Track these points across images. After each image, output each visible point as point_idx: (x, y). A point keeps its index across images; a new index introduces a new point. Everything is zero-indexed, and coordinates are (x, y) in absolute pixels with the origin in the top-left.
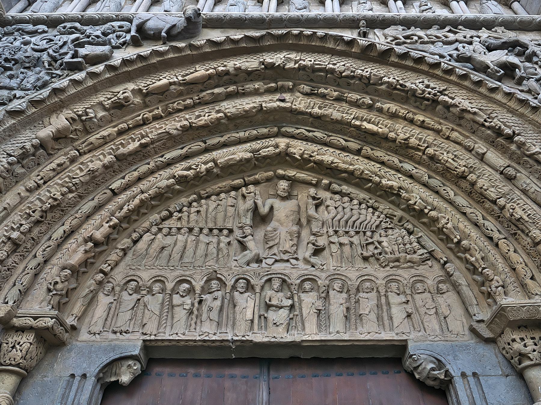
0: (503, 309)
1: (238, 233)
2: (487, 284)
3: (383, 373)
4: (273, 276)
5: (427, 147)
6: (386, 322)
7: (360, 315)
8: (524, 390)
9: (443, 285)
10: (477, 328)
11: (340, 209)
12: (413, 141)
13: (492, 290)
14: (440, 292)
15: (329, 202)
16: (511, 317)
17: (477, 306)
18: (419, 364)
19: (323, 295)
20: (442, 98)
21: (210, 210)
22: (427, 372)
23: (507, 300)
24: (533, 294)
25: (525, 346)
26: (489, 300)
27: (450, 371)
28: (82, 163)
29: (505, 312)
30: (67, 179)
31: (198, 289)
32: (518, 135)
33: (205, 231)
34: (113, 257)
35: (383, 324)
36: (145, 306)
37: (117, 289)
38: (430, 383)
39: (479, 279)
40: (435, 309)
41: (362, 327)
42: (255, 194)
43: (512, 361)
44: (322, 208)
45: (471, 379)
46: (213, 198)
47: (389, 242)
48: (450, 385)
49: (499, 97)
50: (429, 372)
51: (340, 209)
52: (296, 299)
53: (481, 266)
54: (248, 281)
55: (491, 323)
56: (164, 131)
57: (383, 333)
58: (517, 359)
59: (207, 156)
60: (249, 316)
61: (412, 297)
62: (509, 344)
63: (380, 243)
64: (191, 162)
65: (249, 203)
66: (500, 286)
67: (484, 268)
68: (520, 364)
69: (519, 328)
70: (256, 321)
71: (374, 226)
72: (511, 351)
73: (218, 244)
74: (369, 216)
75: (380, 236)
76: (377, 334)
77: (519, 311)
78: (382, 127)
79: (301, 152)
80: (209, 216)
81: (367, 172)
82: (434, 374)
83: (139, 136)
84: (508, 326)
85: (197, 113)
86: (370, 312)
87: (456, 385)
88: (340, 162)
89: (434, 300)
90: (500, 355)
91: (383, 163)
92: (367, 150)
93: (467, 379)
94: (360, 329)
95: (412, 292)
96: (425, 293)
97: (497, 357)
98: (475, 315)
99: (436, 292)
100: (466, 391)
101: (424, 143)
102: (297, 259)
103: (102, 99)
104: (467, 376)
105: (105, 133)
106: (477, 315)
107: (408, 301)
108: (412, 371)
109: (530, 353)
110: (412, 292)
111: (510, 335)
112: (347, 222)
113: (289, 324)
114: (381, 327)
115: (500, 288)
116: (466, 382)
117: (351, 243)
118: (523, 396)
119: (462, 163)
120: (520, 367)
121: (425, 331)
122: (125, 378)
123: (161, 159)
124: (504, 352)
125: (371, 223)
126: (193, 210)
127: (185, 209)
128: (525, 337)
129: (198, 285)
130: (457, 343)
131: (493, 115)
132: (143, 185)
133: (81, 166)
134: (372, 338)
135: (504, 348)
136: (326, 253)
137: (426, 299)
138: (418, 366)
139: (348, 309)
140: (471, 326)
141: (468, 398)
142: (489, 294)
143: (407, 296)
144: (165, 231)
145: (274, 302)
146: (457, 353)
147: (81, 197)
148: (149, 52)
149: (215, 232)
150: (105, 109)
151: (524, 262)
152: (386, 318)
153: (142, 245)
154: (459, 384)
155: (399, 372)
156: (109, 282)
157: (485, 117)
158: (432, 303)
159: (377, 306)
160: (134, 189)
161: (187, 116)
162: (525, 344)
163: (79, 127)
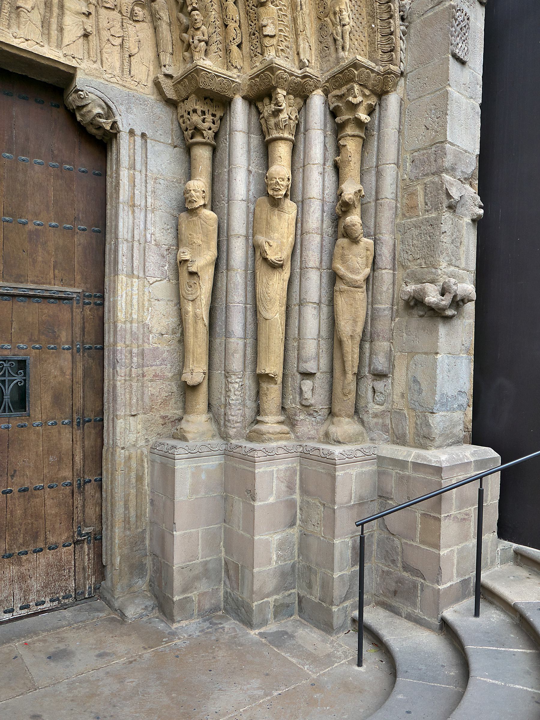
0: (197, 70)
2: (191, 31)
3: (36, 101)
6: (54, 33)
7: (18, 8)
8: (186, 165)
9: (140, 9)
10: (162, 83)
13: (193, 42)
14: (135, 18)
16: (201, 84)
17: (171, 56)
18: (84, 104)
22: (92, 117)
23: (205, 62)
24: (233, 66)
25: (204, 121)
26: (186, 53)
27: (118, 123)
29: (198, 76)
35: (49, 34)
38: (93, 131)
39: (185, 20)
40: (121, 38)
41: (19, 27)
43: (186, 133)
45: (138, 139)
48: (114, 139)
50: (94, 118)
53: (192, 4)
55: (179, 82)
57: (46, 46)
58: (190, 132)
61: (97, 11)
62: (189, 114)
66: (203, 41)
67: (194, 9)
68: (191, 138)
69: (205, 99)
72: (188, 122)
76: (37, 46)
77: (212, 80)
82: (99, 122)
84: (194, 93)
86: (33, 9)
87: (121, 141)
89: (123, 26)
90: (175, 122)
93: (134, 138)
94: (14, 29)
95: (98, 3)
96: (115, 12)
97: (172, 124)
98: (165, 66)
99: (129, 16)
100: (129, 150)
104: (135, 135)
106: (167, 66)
107: (90, 14)
108: (74, 109)
109: (205, 130)
110: (98, 3)
111: (192, 104)
114: (45, 37)
115: (203, 43)
116: (132, 142)
118: (183, 171)
120: (191, 141)
121: (102, 64)
124: (181, 121)
128: (207, 112)
130: (135, 93)
134: (30, 49)
135: (182, 116)
137: (113, 20)
138: (84, 106)
140: (157, 78)
141: (129, 158)
142: (189, 45)
143: (90, 5)
146: (132, 105)
151: (240, 21)
152: (54, 26)
154: (124, 140)
155: (58, 106)
158: (120, 30)
159: (45, 4)
162: (204, 119)
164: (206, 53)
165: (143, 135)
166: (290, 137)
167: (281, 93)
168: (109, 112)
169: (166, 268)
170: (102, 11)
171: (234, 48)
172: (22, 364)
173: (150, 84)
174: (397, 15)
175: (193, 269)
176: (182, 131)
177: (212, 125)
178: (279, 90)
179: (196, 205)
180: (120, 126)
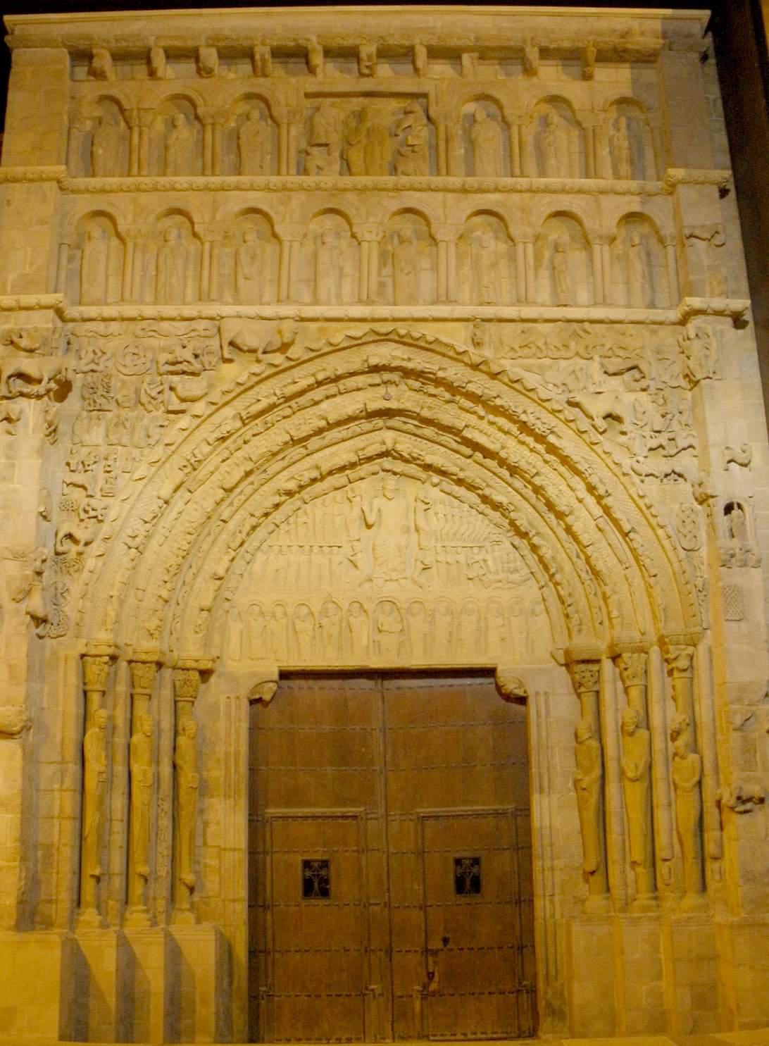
1: (346, 550)
4: (384, 599)
5: (537, 474)
11: (449, 517)
12: (523, 465)
15: (440, 508)
19: (429, 619)
20: (552, 439)
21: (317, 522)
28: (196, 502)
30: (188, 525)
31: (317, 615)
32: (609, 495)
33: (316, 549)
34: (232, 584)
36: (272, 633)
37: (243, 615)
42: (361, 497)
44: (431, 512)
46: (318, 501)
47: (494, 559)
49: (600, 451)
51: (449, 517)
52: (405, 622)
54: (361, 605)
56: (265, 450)
59: (309, 462)
60: (365, 642)
63: (485, 561)
64: (292, 469)
65: (356, 512)
70: (371, 648)
71: (482, 539)
73: (330, 562)
74: (479, 523)
75: (487, 552)
78: (495, 441)
79: (409, 450)
80: (317, 528)
81: (478, 480)
83: (242, 459)
85: (297, 423)
88: (451, 465)
91: (494, 474)
92: (479, 456)
101: (534, 467)
102: (405, 578)
103: (205, 435)
105: (211, 467)
112: (455, 534)
113: (399, 650)
117: (458, 562)
119: (564, 501)
122: (267, 697)
123: (263, 476)
125: (479, 536)
126: (300, 520)
127: (291, 520)
129: (316, 609)
131: (593, 466)
132: (248, 507)
133: (194, 505)
136: (434, 570)
139: (451, 633)
144: (276, 549)
145: (383, 629)
147: (198, 536)
148: (246, 376)
149: (326, 550)
150: (209, 444)
153: (257, 567)
156: (233, 607)
157: (586, 466)
160: (242, 512)
161: (287, 428)
163: (189, 469)
164: (580, 631)
165: (546, 693)
166: (639, 683)
167: (626, 656)
168: (521, 685)
169: (570, 785)
170: (513, 618)
171: (597, 625)
172: (476, 861)
173: (548, 656)
174: (694, 591)
175: (584, 786)
176: (574, 684)
177: (591, 679)
178: (624, 655)
179: (584, 739)
180: (528, 691)
